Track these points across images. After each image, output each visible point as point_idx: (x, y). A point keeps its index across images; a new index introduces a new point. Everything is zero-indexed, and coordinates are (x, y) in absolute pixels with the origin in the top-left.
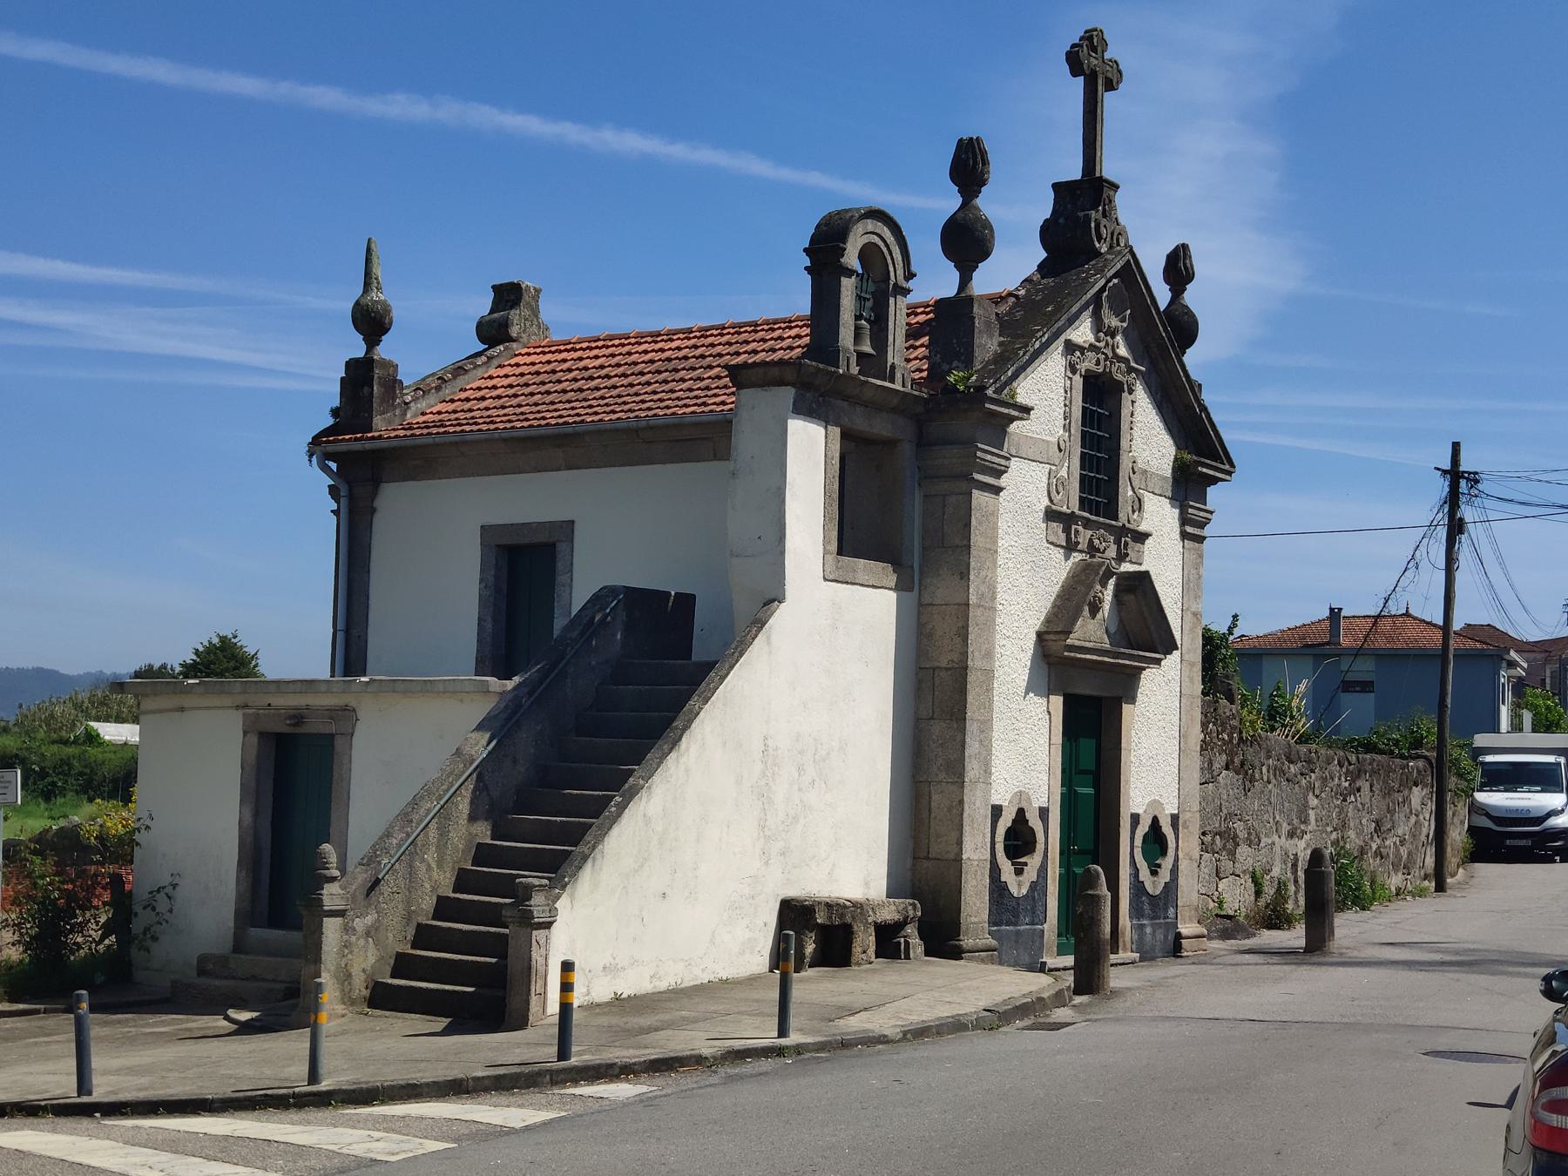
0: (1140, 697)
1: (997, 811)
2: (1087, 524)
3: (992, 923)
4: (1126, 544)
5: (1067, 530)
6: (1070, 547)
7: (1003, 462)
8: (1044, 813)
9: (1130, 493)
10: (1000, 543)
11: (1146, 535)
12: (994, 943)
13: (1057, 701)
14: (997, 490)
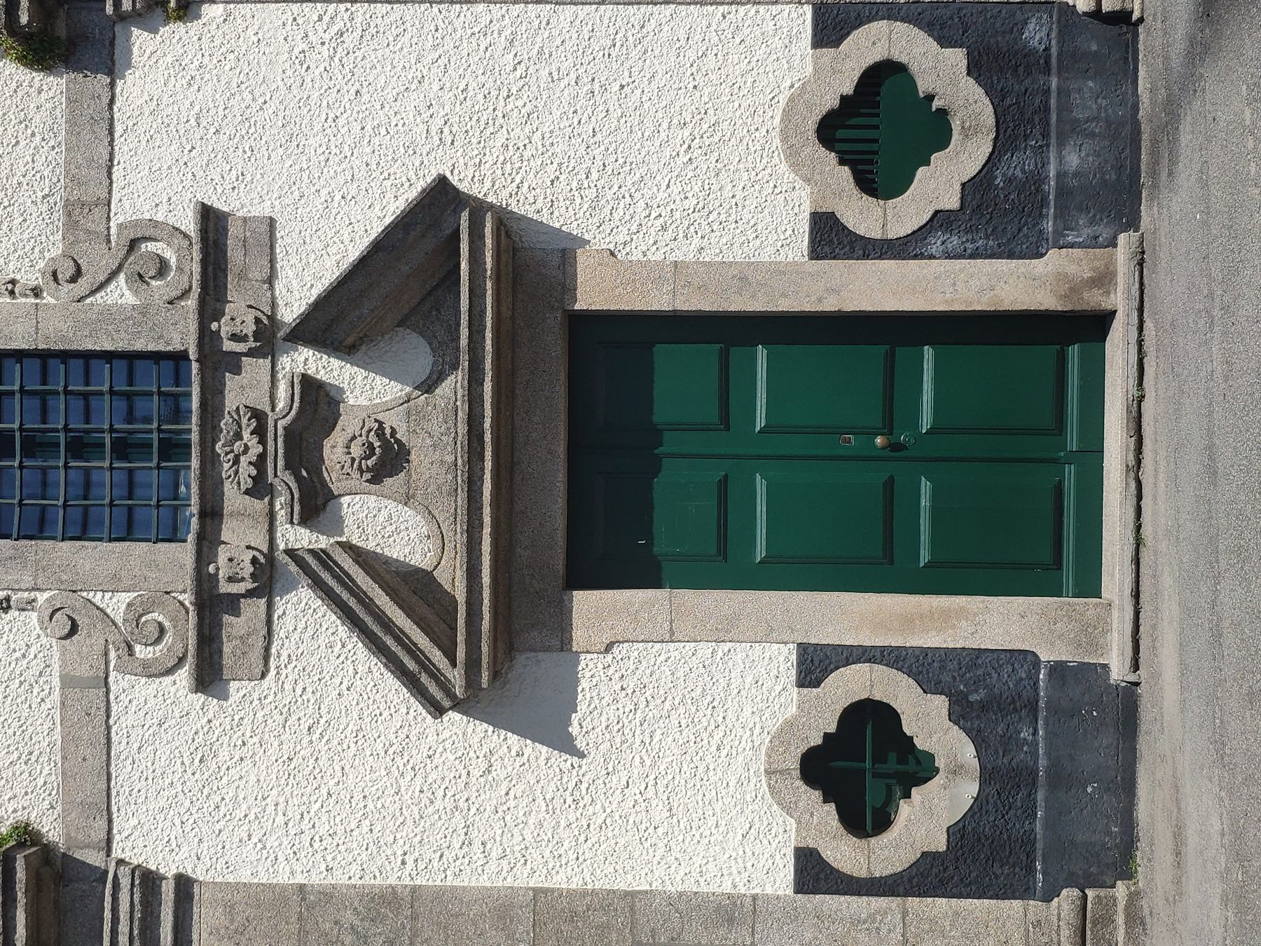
0: (563, 218)
1: (813, 873)
2: (212, 514)
3: (1023, 891)
4: (234, 337)
5: (232, 604)
6: (267, 578)
7: (125, 882)
8: (814, 665)
9: (121, 293)
10: (283, 877)
11: (212, 223)
12: (1069, 895)
13: (585, 602)
14: (184, 885)
